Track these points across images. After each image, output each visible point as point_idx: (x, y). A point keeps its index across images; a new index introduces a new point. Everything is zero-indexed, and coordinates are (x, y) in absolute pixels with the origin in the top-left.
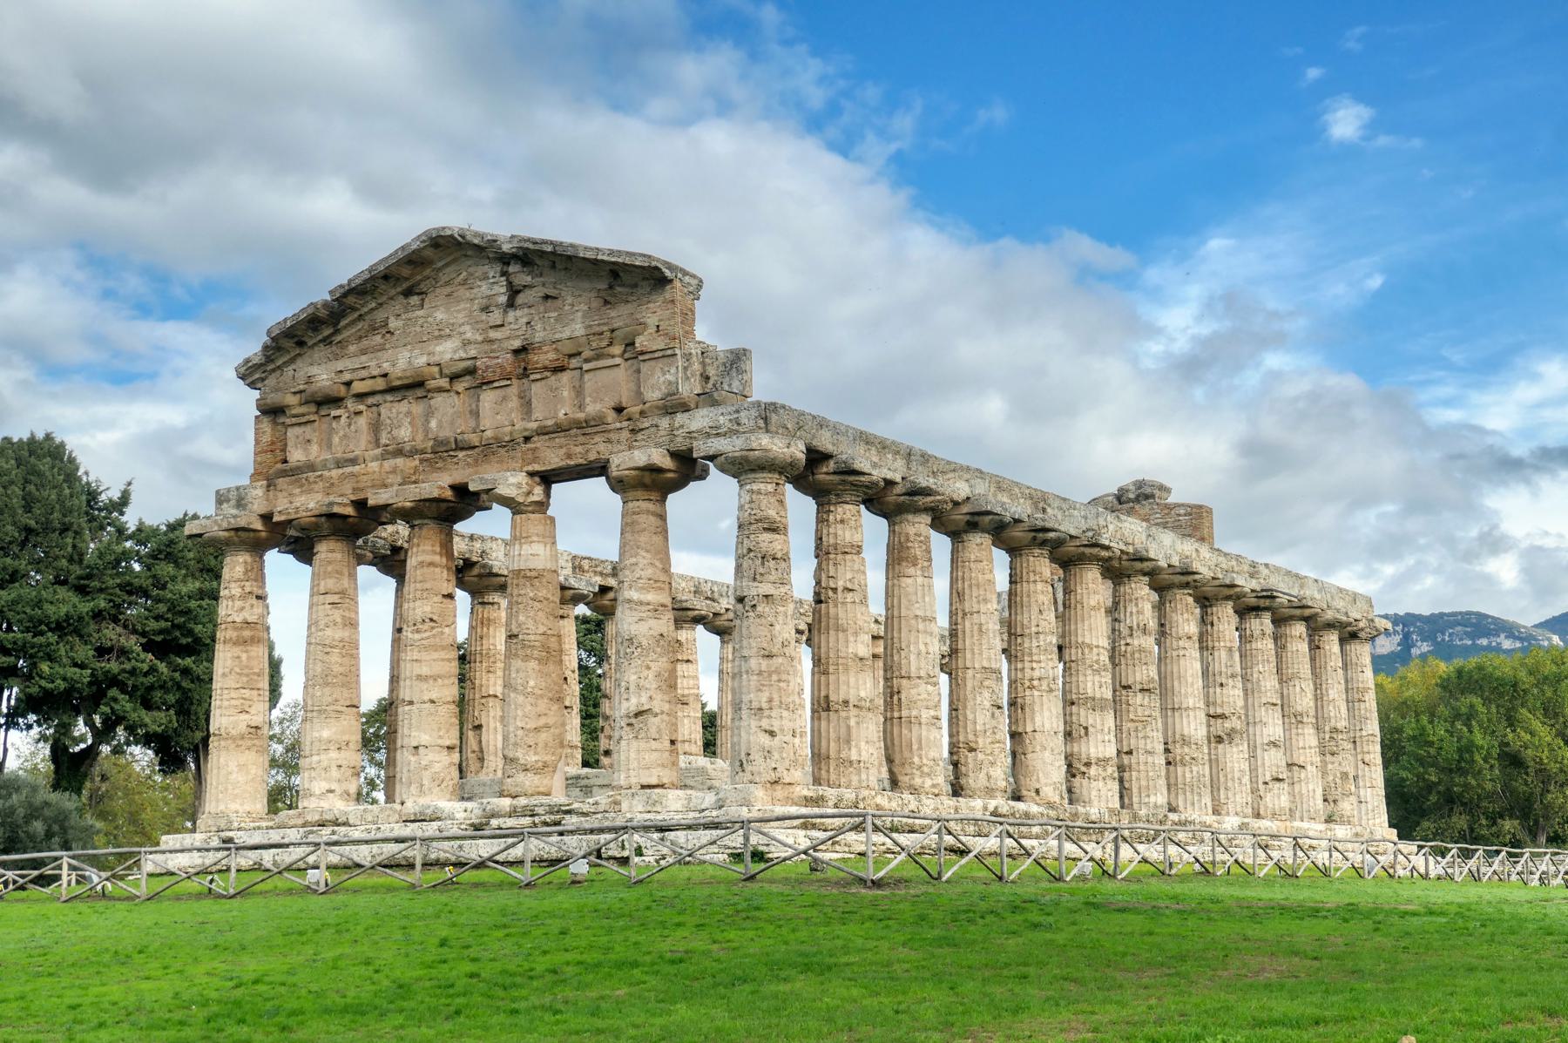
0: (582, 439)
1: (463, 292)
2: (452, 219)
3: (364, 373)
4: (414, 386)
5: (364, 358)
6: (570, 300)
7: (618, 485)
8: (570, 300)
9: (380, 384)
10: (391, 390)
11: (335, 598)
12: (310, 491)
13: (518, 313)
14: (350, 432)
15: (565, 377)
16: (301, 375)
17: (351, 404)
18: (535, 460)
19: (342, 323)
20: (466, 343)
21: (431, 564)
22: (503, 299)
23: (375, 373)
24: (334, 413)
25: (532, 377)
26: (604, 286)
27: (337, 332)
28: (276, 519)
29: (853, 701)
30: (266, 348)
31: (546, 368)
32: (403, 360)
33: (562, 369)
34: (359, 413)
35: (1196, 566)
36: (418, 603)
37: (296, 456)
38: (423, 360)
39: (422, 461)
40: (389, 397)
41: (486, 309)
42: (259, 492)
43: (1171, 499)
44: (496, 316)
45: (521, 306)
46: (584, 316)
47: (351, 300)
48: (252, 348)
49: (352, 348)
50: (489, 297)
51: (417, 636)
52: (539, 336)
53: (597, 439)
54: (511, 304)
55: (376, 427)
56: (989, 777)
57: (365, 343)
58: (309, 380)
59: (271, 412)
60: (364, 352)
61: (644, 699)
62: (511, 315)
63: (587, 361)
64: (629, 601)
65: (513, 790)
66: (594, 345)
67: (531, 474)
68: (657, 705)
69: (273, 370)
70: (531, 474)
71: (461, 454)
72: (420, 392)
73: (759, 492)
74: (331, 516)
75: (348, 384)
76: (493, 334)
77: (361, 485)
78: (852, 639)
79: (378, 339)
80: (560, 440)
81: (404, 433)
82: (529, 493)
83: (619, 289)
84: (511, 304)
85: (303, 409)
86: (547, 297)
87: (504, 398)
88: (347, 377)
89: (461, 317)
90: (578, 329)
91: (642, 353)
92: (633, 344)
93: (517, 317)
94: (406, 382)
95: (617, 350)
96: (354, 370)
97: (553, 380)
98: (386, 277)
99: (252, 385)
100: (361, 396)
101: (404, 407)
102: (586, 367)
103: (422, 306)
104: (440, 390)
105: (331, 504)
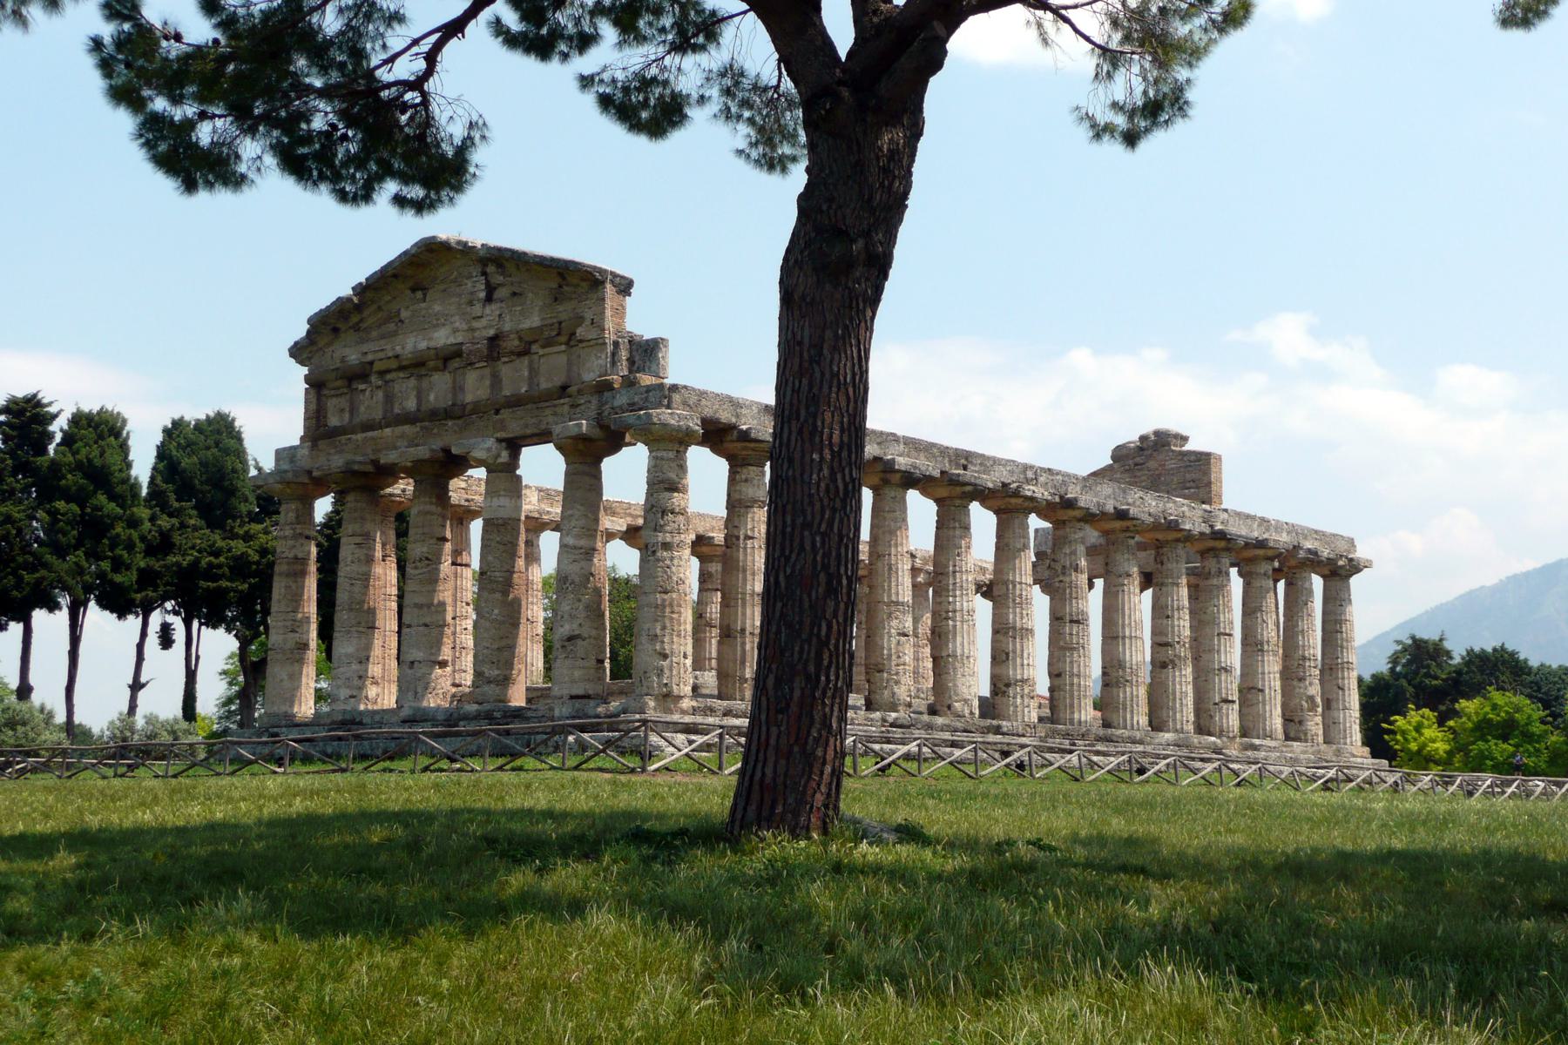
3: (381, 355)
4: (418, 366)
5: (382, 342)
7: (559, 448)
9: (394, 364)
10: (401, 368)
11: (358, 540)
12: (341, 452)
13: (494, 306)
14: (370, 403)
15: (526, 360)
16: (337, 355)
17: (373, 378)
18: (503, 428)
19: (366, 313)
20: (455, 331)
21: (428, 513)
22: (482, 295)
26: (555, 285)
27: (361, 320)
28: (315, 474)
29: (749, 629)
30: (309, 332)
31: (512, 353)
32: (412, 344)
34: (379, 387)
35: (1133, 511)
37: (334, 421)
38: (423, 345)
41: (471, 303)
42: (305, 452)
43: (1188, 447)
44: (477, 309)
47: (369, 295)
48: (300, 330)
49: (374, 334)
52: (507, 327)
53: (548, 412)
54: (489, 299)
55: (389, 399)
56: (894, 694)
58: (343, 360)
59: (315, 385)
60: (383, 337)
61: (575, 626)
62: (488, 310)
63: (543, 347)
65: (480, 699)
67: (499, 440)
68: (585, 632)
70: (499, 440)
73: (662, 459)
74: (354, 473)
75: (371, 363)
76: (476, 324)
78: (749, 577)
79: (392, 326)
80: (520, 412)
81: (411, 404)
82: (498, 456)
84: (489, 299)
85: (339, 383)
86: (514, 294)
87: (482, 377)
88: (370, 357)
90: (534, 321)
91: (581, 341)
92: (574, 334)
93: (492, 310)
95: (563, 339)
98: (395, 276)
99: (302, 363)
100: (382, 373)
101: (412, 382)
102: (541, 352)
105: (354, 462)
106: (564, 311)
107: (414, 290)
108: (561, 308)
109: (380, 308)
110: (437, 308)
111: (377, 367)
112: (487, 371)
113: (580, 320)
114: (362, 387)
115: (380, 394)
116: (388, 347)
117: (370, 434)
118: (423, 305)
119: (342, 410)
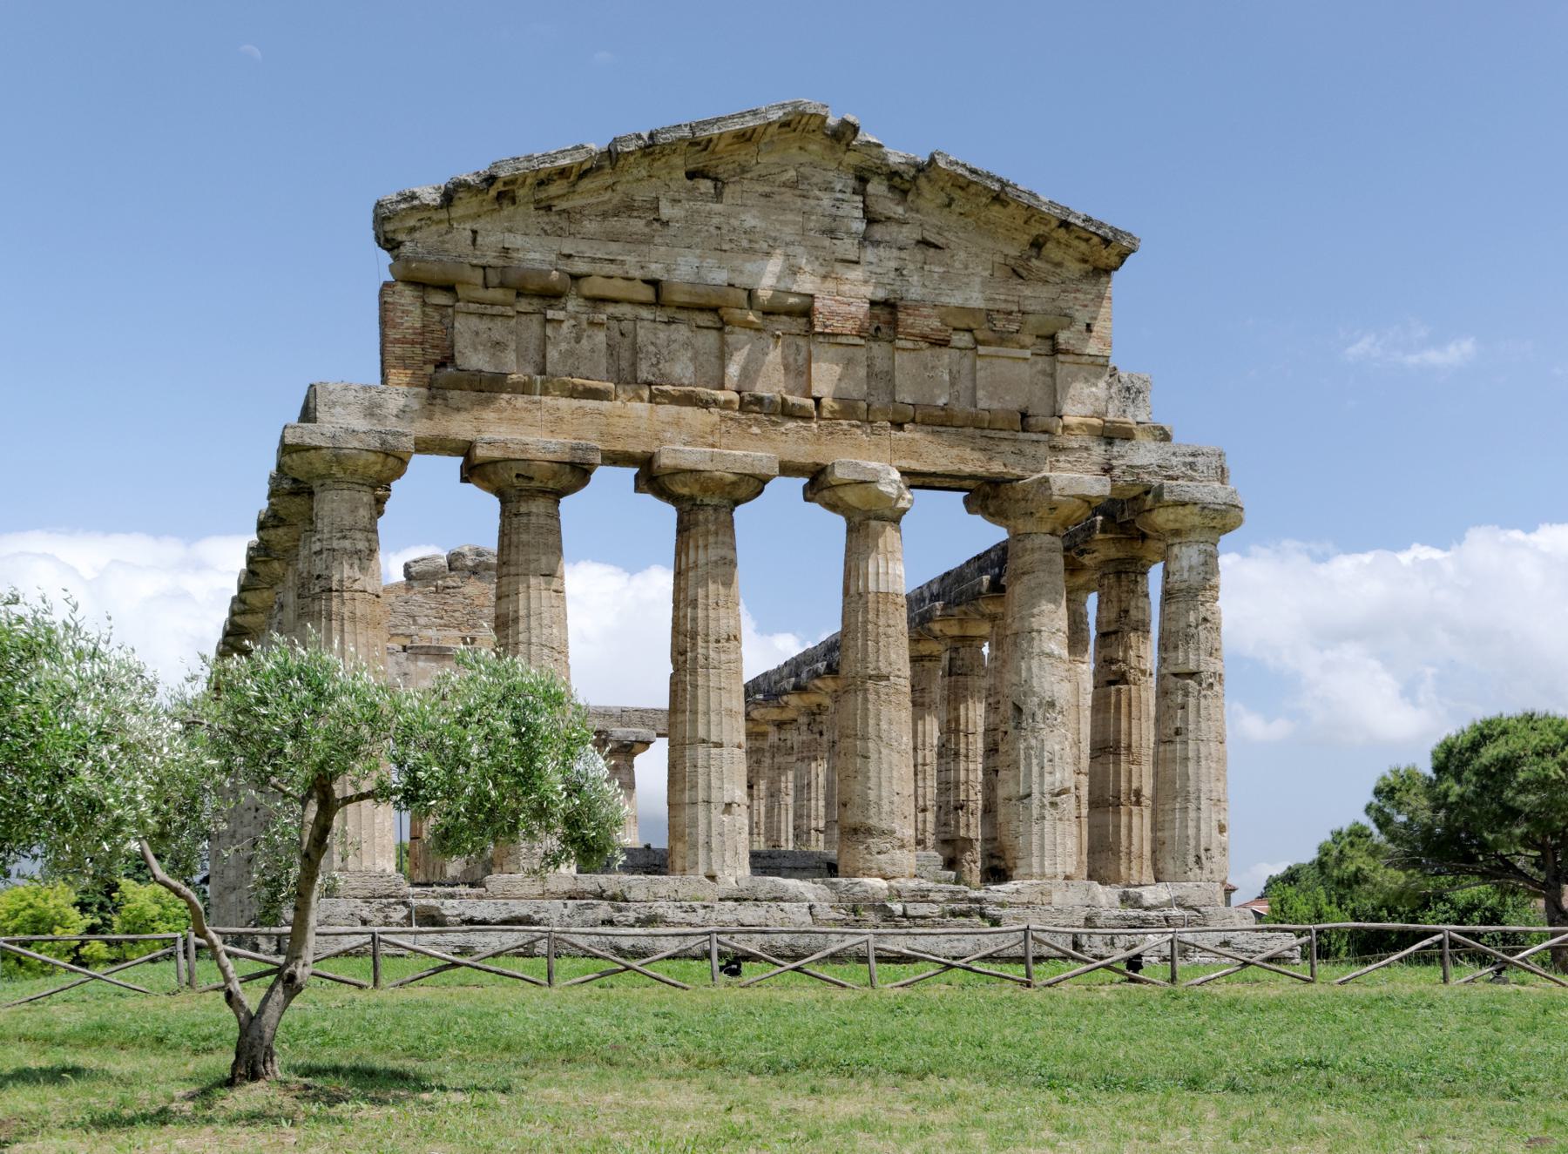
0: (983, 443)
1: (788, 195)
2: (811, 101)
3: (609, 269)
5: (614, 247)
6: (962, 255)
8: (962, 255)
10: (658, 302)
13: (881, 251)
15: (946, 355)
17: (573, 304)
23: (637, 274)
24: (550, 314)
25: (900, 343)
26: (1013, 251)
31: (924, 337)
32: (685, 268)
33: (944, 343)
36: (722, 611)
37: (475, 359)
38: (721, 277)
39: (723, 419)
40: (645, 313)
41: (831, 233)
45: (889, 245)
46: (983, 283)
50: (835, 218)
51: (723, 657)
52: (915, 292)
57: (614, 224)
62: (870, 254)
64: (1050, 655)
66: (999, 325)
69: (441, 221)
70: (903, 473)
71: (791, 425)
72: (704, 319)
75: (576, 278)
77: (618, 431)
79: (638, 225)
83: (1035, 263)
84: (865, 240)
85: (496, 294)
86: (924, 243)
88: (580, 267)
89: (788, 233)
90: (976, 299)
91: (1067, 352)
94: (702, 301)
96: (593, 260)
97: (928, 353)
100: (598, 301)
101: (682, 332)
102: (981, 350)
103: (718, 196)
104: (748, 325)
106: (1034, 296)
107: (691, 175)
108: (1028, 292)
109: (611, 187)
110: (750, 220)
111: (588, 287)
112: (861, 354)
113: (1068, 319)
114: (560, 315)
115: (600, 337)
116: (631, 259)
117: (590, 404)
118: (718, 207)
119: (498, 345)
